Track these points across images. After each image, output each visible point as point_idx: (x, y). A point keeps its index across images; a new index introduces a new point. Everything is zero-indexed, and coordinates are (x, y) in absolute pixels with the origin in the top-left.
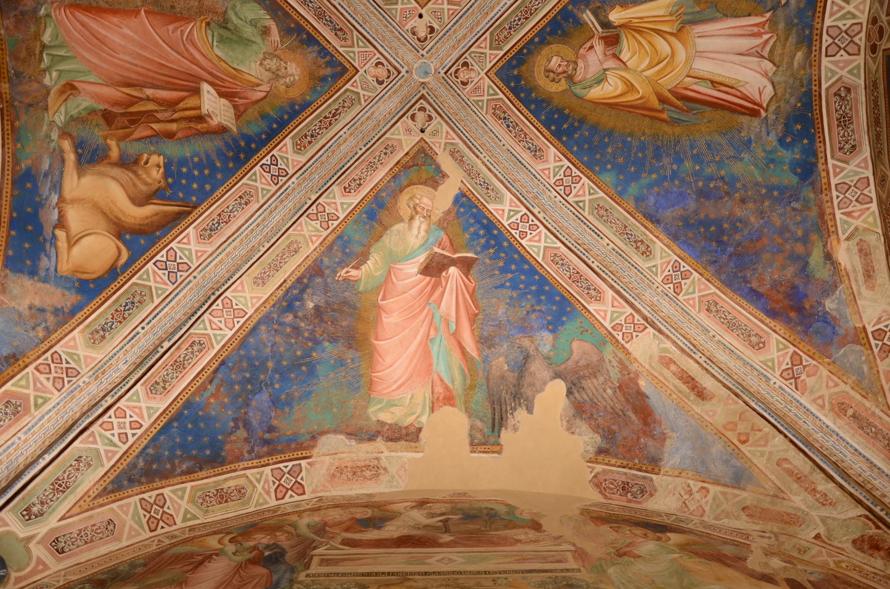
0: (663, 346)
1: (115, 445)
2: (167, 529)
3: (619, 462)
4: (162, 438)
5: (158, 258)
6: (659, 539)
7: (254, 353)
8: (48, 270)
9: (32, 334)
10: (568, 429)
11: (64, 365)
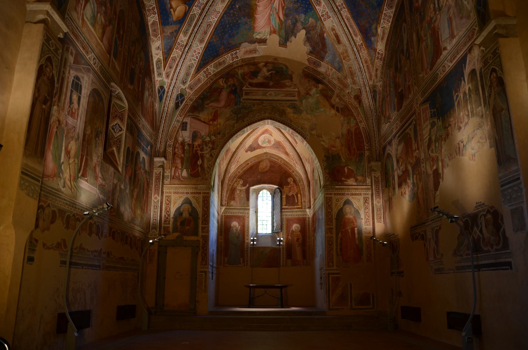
0: (333, 24)
1: (196, 60)
2: (210, 76)
3: (315, 56)
4: (205, 54)
5: (196, 4)
6: (316, 87)
7: (223, 23)
8: (171, 21)
9: (172, 40)
10: (304, 44)
11: (181, 45)
